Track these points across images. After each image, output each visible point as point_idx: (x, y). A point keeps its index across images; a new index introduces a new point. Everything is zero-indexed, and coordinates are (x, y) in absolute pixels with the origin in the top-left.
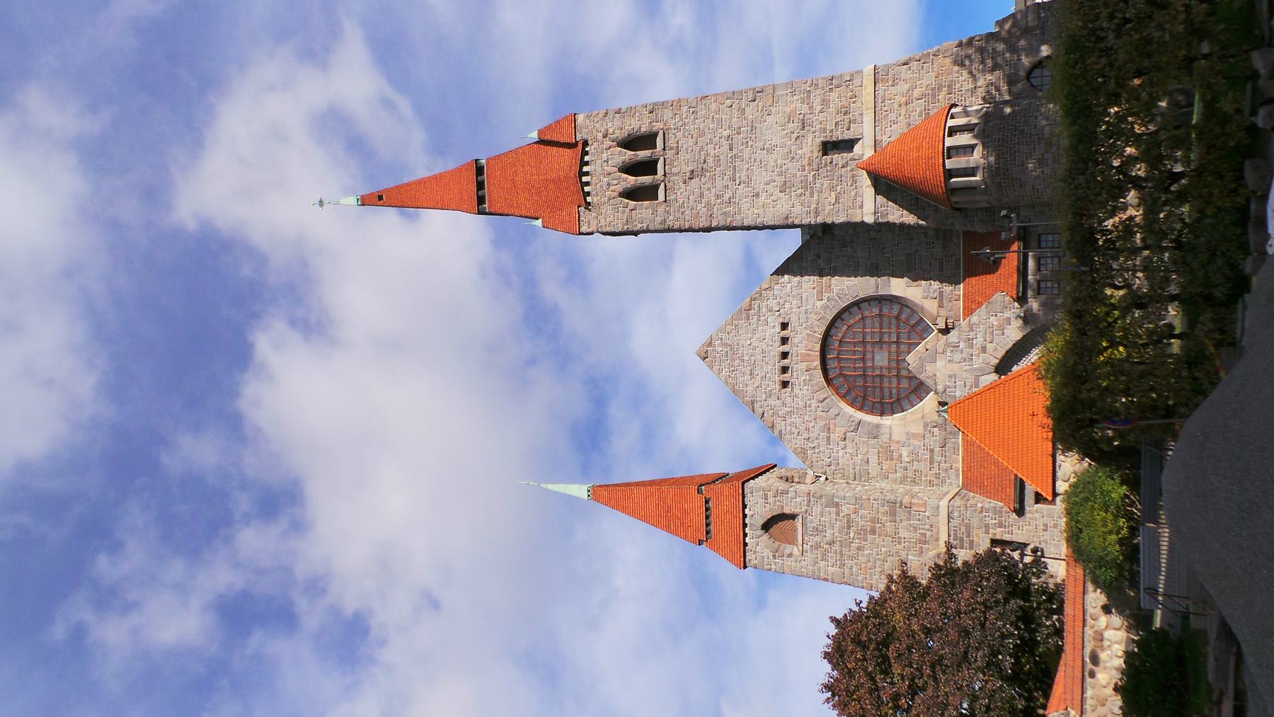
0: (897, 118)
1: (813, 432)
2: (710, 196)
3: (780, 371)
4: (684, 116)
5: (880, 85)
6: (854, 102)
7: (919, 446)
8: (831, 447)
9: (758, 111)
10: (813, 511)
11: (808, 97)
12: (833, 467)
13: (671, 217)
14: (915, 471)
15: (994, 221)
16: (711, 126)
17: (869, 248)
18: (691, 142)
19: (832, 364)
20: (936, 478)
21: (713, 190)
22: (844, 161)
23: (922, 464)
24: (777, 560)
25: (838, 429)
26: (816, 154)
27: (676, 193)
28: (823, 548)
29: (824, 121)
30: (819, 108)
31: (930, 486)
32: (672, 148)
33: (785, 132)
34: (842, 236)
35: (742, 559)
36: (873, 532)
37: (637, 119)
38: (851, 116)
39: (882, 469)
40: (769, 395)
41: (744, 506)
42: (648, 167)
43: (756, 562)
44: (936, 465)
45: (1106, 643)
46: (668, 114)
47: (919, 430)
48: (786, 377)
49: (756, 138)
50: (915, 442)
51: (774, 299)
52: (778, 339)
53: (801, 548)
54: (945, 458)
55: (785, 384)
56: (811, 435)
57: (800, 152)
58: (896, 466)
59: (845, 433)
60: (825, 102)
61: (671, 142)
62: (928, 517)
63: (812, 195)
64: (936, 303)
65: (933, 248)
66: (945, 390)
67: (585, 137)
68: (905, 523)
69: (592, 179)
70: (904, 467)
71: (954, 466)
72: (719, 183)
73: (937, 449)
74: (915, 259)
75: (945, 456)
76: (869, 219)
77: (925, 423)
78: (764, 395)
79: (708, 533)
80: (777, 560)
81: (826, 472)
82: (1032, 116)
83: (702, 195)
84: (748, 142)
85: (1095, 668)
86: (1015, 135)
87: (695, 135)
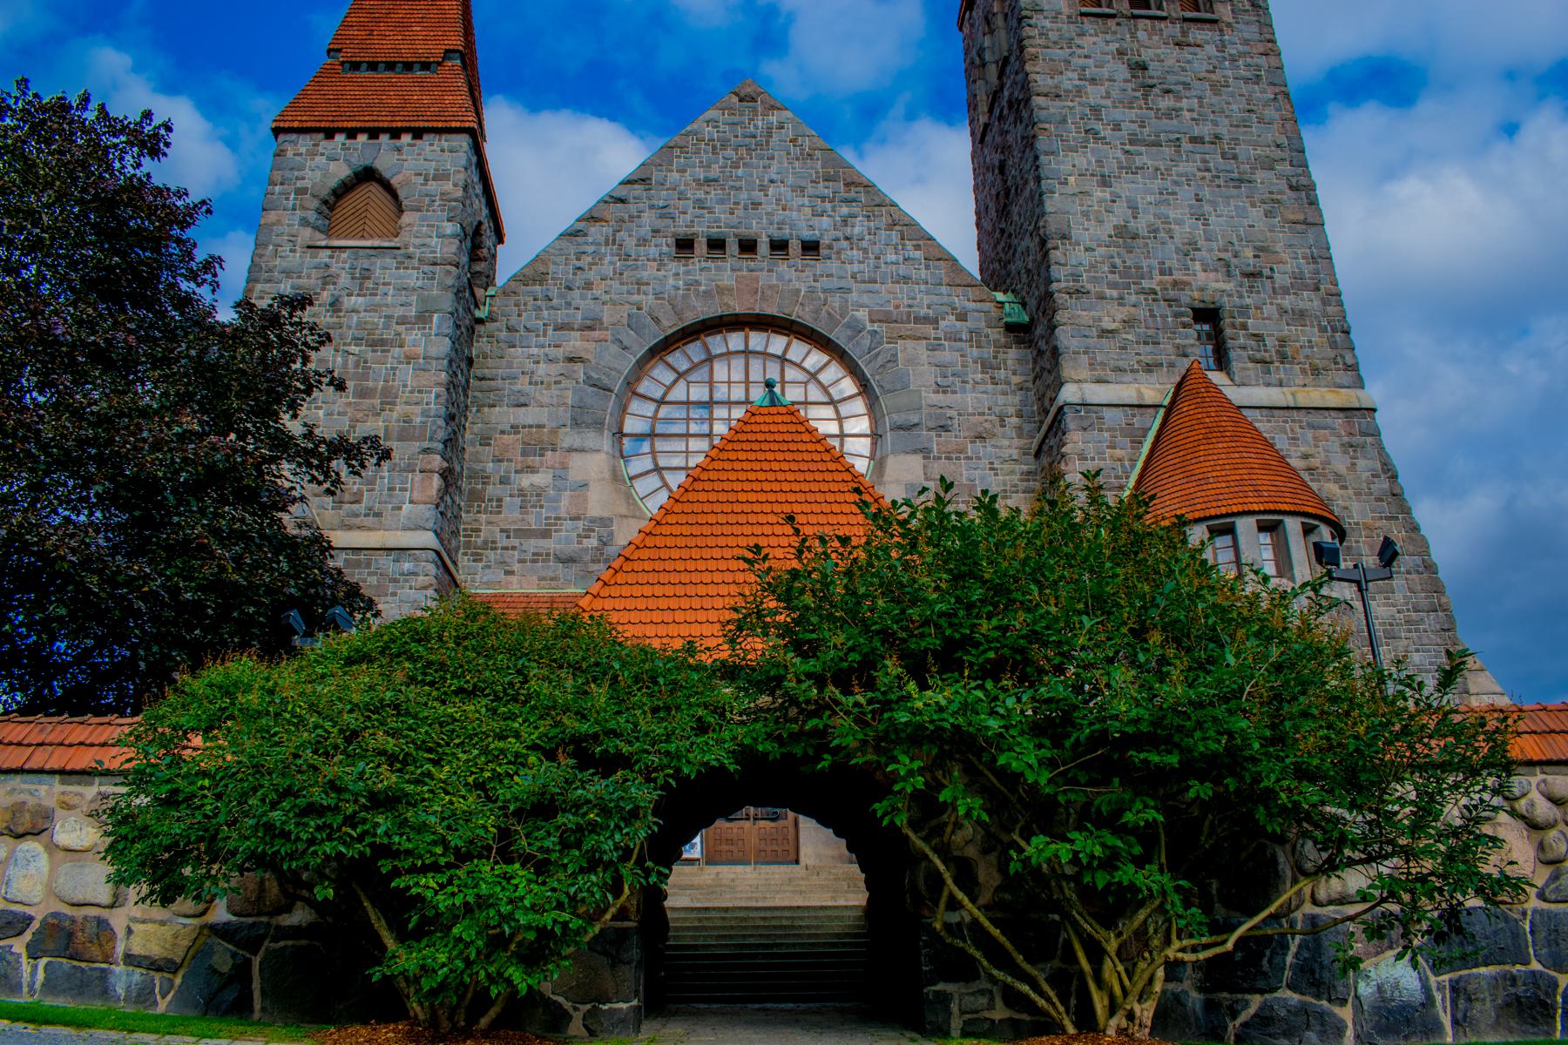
3: (715, 237)
4: (1249, 60)
5: (1338, 421)
6: (1303, 371)
8: (550, 332)
10: (410, 271)
11: (1306, 288)
12: (504, 335)
13: (1047, 24)
14: (500, 500)
16: (1234, 107)
17: (983, 414)
18: (1201, 67)
20: (486, 542)
21: (1108, 103)
23: (517, 515)
26: (1196, 294)
27: (1097, 35)
28: (323, 289)
29: (1262, 313)
32: (1184, 33)
33: (1235, 241)
34: (1005, 364)
35: (296, 125)
38: (1277, 364)
39: (503, 432)
40: (665, 213)
41: (418, 134)
43: (290, 154)
44: (515, 542)
46: (1251, 32)
47: (595, 508)
48: (701, 247)
49: (1219, 186)
51: (869, 229)
55: (685, 245)
57: (1198, 266)
58: (510, 460)
59: (579, 360)
60: (1300, 316)
61: (1197, 34)
62: (400, 508)
63: (1113, 286)
70: (509, 478)
71: (514, 579)
72: (1117, 114)
73: (548, 545)
76: (1069, 393)
77: (611, 520)
78: (661, 203)
79: (355, 66)
80: (293, 196)
84: (1208, 170)
87: (1213, 77)
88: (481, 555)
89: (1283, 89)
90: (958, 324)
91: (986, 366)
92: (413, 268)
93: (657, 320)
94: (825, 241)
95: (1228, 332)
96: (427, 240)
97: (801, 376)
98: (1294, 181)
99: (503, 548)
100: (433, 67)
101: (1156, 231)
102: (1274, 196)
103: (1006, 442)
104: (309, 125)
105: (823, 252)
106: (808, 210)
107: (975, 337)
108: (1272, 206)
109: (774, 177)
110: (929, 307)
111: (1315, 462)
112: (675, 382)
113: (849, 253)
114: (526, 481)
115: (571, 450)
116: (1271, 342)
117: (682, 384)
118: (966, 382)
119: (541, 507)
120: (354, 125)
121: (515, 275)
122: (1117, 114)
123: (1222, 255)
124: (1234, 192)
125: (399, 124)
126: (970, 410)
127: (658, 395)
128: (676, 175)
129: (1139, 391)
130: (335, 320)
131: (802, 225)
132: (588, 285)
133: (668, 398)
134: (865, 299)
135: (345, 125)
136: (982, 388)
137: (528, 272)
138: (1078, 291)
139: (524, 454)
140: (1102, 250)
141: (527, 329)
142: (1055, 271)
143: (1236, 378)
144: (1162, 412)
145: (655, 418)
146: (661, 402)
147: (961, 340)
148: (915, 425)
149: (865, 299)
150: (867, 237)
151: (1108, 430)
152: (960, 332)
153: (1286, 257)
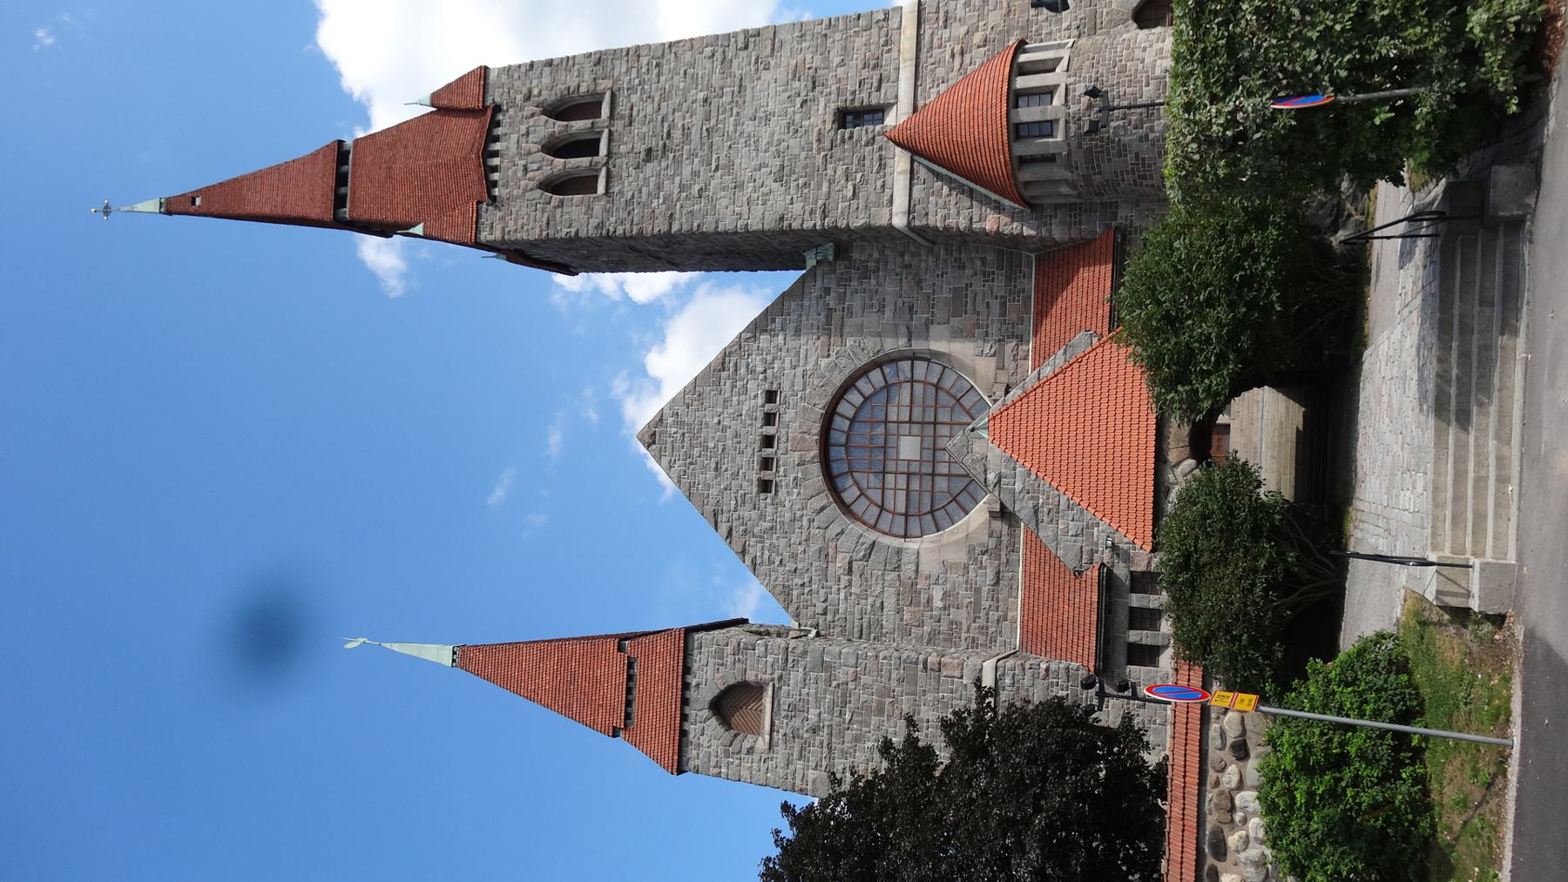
0: (947, 74)
1: (803, 560)
2: (672, 187)
4: (644, 70)
5: (927, 30)
8: (829, 584)
9: (750, 64)
13: (613, 219)
14: (951, 623)
15: (1081, 224)
19: (837, 452)
21: (677, 179)
22: (871, 136)
24: (731, 760)
25: (840, 556)
26: (828, 126)
28: (802, 738)
30: (837, 60)
31: (972, 648)
32: (622, 117)
34: (863, 261)
36: (880, 710)
37: (576, 73)
38: (882, 71)
41: (687, 670)
42: (588, 146)
43: (697, 762)
44: (983, 613)
45: (1238, 816)
47: (962, 557)
48: (767, 475)
52: (760, 415)
53: (767, 737)
56: (800, 566)
57: (806, 123)
59: (850, 563)
61: (622, 108)
62: (966, 685)
63: (819, 186)
64: (992, 362)
65: (993, 281)
66: (999, 481)
67: (498, 100)
68: (930, 697)
69: (501, 162)
72: (687, 171)
74: (966, 297)
76: (899, 221)
78: (733, 502)
80: (731, 760)
81: (818, 625)
83: (659, 187)
85: (1219, 865)
87: (656, 99)
89: (667, 46)
90: (832, 294)
91: (865, 275)
92: (789, 674)
93: (823, 508)
94: (767, 387)
95: (857, 104)
96: (769, 664)
97: (867, 408)
98: (740, 45)
100: (632, 660)
101: (778, 152)
102: (753, 61)
103: (923, 265)
104: (676, 748)
105: (775, 387)
106: (742, 397)
107: (843, 282)
108: (761, 65)
109: (716, 420)
110: (819, 315)
111: (957, 49)
112: (867, 497)
113: (776, 370)
114: (938, 603)
115: (917, 571)
116: (865, 73)
117: (870, 493)
118: (877, 290)
120: (678, 715)
121: (784, 607)
122: (687, 171)
123: (798, 105)
124: (749, 91)
125: (680, 683)
126: (898, 289)
127: (876, 510)
128: (713, 492)
129: (899, 173)
130: (826, 729)
131: (754, 403)
132: (794, 556)
133: (880, 503)
134: (812, 360)
135: (678, 722)
136: (881, 280)
137: (782, 598)
138: (824, 211)
139: (918, 605)
140: (792, 191)
141: (825, 601)
142: (808, 225)
143: (892, 101)
144: (916, 158)
145: (894, 513)
146: (882, 508)
147: (845, 293)
148: (908, 328)
149: (812, 360)
150: (764, 356)
152: (839, 294)
153: (800, 57)
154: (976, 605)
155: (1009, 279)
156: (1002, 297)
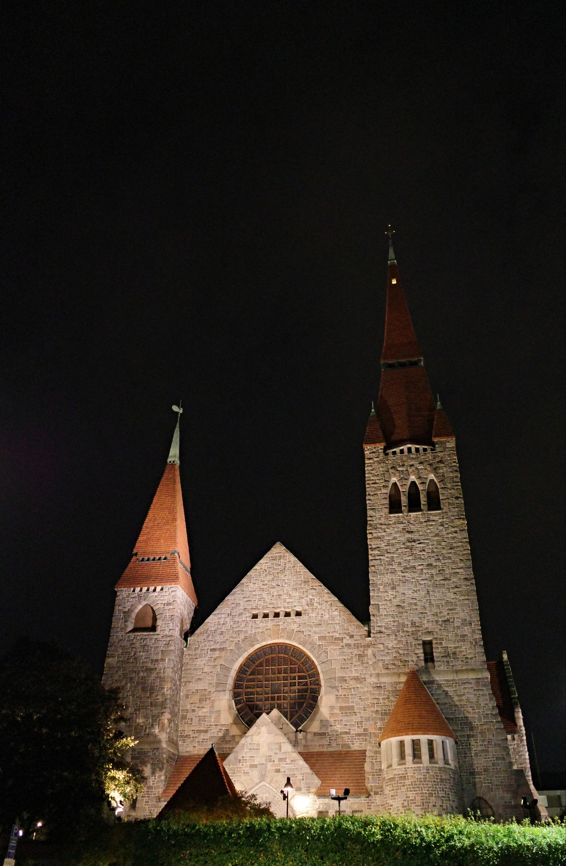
7: (210, 721)
14: (192, 719)
29: (448, 638)
44: (196, 735)
50: (213, 720)
54: (202, 742)
65: (358, 727)
75: (203, 742)
82: (443, 803)
86: (428, 790)
88: (185, 740)
99: (193, 737)
119: (205, 721)
151: (387, 691)
154: (199, 731)
155: (359, 735)
156: (350, 732)
